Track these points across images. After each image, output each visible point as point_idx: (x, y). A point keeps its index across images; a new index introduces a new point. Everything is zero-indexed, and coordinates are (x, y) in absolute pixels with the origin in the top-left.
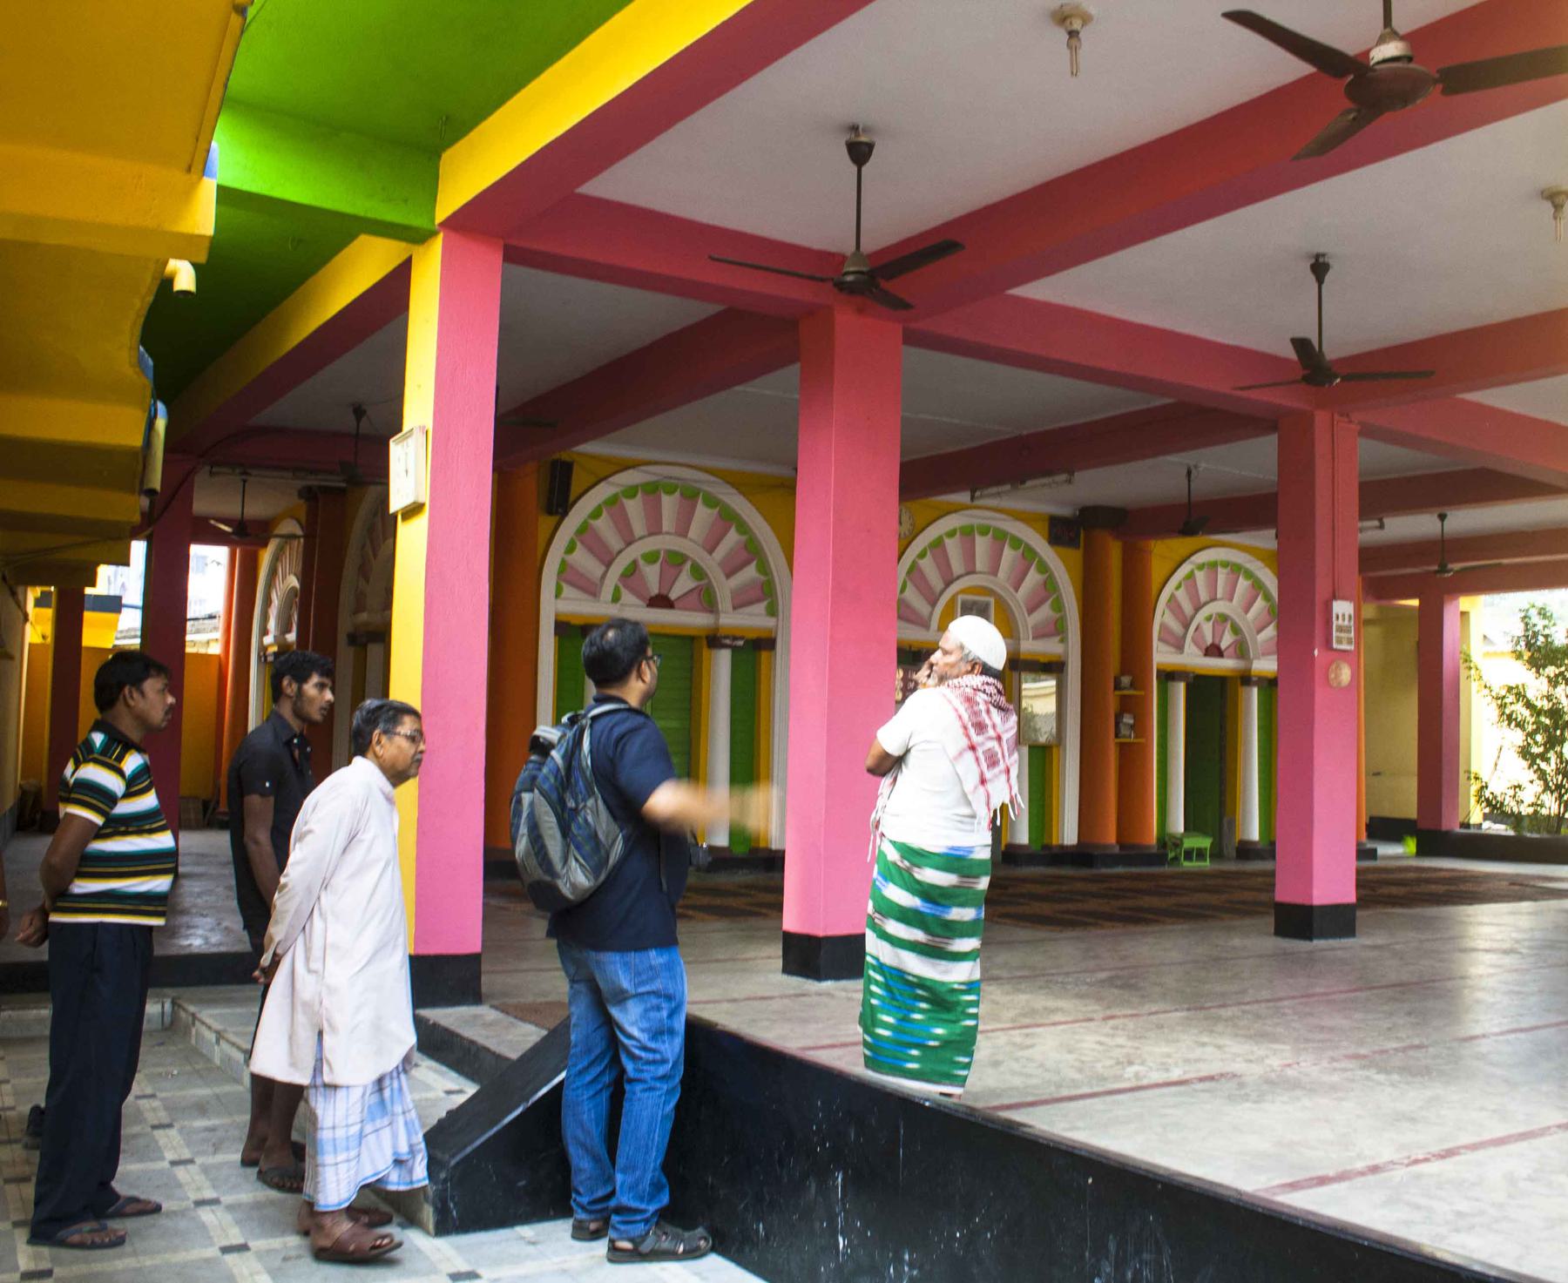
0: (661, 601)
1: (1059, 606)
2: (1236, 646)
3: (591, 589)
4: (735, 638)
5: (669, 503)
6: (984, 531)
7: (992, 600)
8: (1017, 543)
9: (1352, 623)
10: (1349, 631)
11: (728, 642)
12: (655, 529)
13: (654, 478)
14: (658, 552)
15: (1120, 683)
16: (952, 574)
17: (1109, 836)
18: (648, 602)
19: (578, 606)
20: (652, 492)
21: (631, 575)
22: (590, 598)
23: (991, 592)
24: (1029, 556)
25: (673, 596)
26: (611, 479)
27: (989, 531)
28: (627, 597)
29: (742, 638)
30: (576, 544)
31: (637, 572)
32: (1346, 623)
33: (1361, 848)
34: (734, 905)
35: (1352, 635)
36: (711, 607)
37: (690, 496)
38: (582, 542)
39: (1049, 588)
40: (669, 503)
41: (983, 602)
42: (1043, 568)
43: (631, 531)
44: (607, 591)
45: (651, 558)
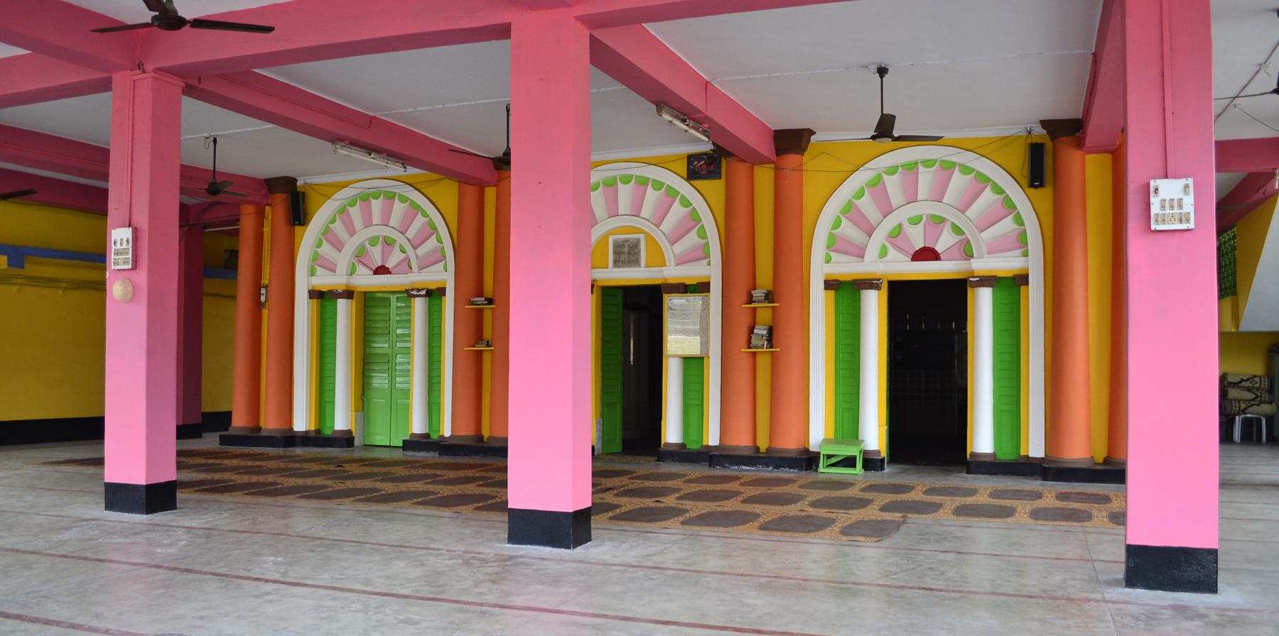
0: (381, 270)
1: (702, 234)
2: (961, 245)
3: (332, 268)
4: (419, 290)
5: (376, 205)
6: (627, 180)
7: (641, 236)
8: (658, 185)
9: (131, 245)
10: (127, 253)
11: (415, 293)
12: (368, 223)
13: (359, 191)
14: (921, 216)
15: (752, 296)
16: (891, 206)
17: (763, 445)
18: (911, 257)
19: (324, 281)
20: (365, 199)
21: (896, 235)
22: (333, 274)
23: (640, 231)
24: (671, 194)
25: (389, 265)
26: (333, 197)
27: (632, 179)
28: (361, 269)
29: (423, 289)
30: (322, 241)
31: (902, 232)
32: (125, 246)
33: (867, 457)
34: (463, 475)
35: (130, 256)
36: (969, 256)
37: (390, 198)
38: (327, 240)
39: (693, 220)
40: (376, 205)
41: (633, 239)
42: (685, 203)
43: (943, 197)
44: (342, 267)
45: (915, 221)
